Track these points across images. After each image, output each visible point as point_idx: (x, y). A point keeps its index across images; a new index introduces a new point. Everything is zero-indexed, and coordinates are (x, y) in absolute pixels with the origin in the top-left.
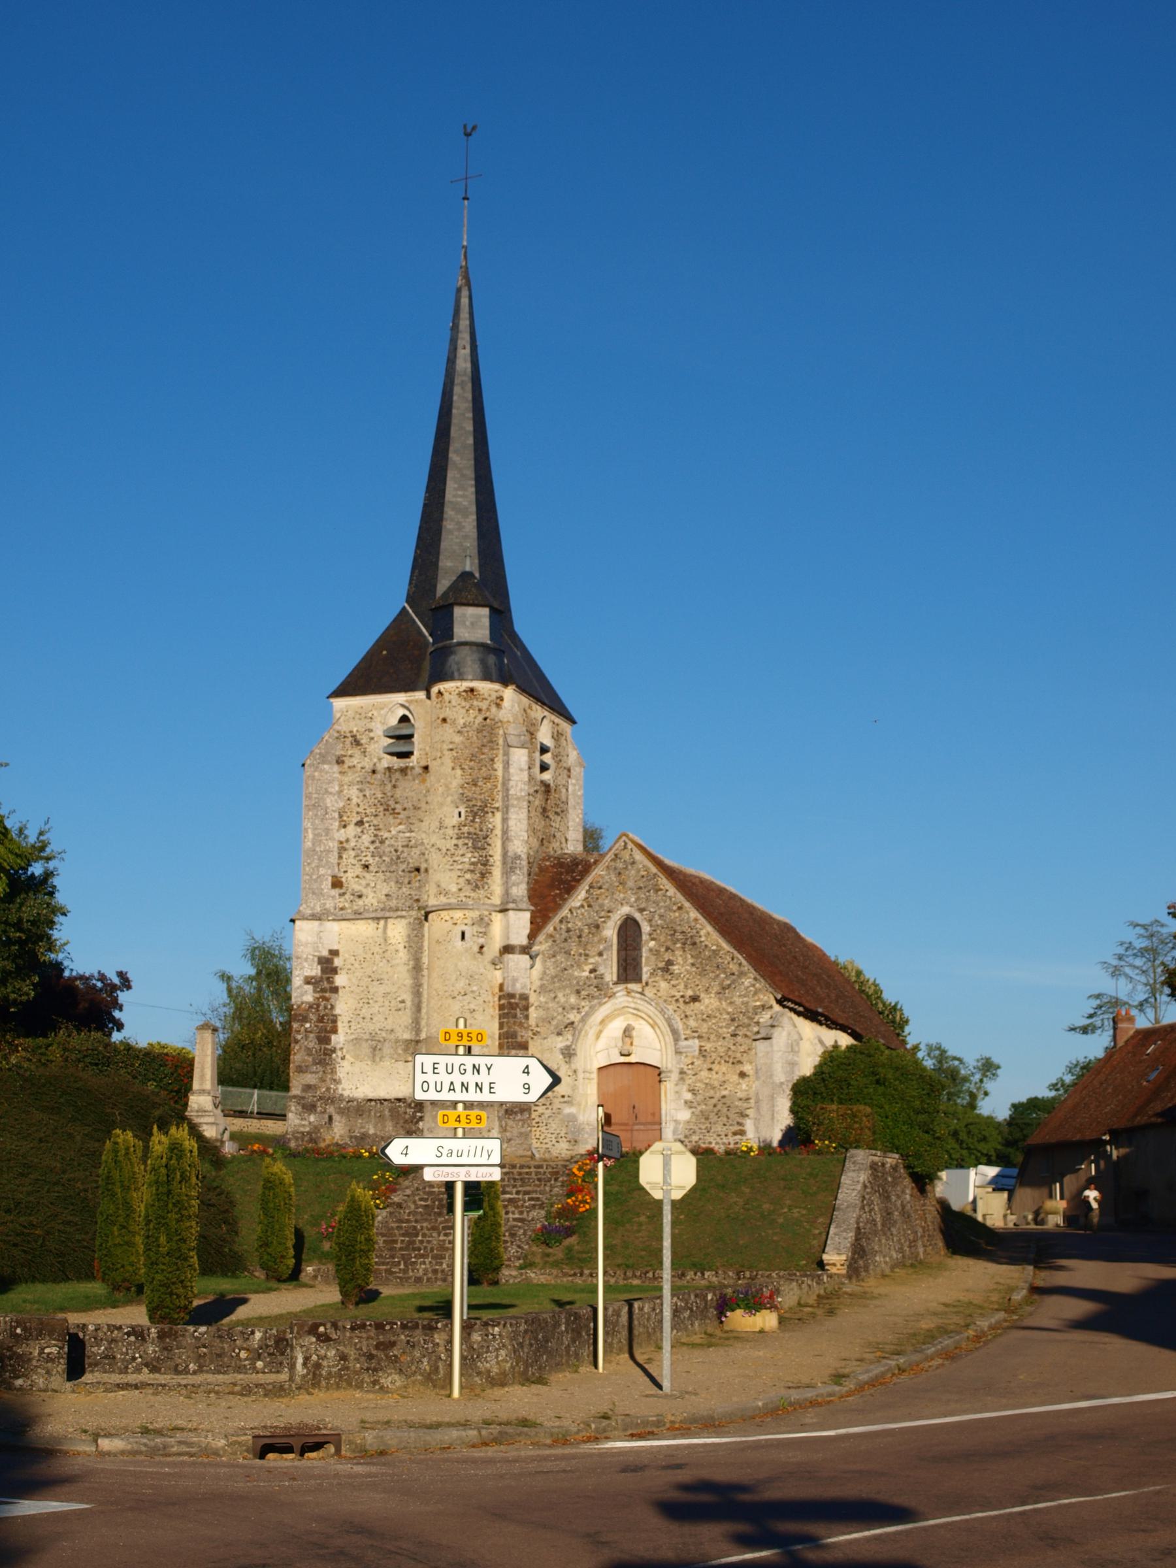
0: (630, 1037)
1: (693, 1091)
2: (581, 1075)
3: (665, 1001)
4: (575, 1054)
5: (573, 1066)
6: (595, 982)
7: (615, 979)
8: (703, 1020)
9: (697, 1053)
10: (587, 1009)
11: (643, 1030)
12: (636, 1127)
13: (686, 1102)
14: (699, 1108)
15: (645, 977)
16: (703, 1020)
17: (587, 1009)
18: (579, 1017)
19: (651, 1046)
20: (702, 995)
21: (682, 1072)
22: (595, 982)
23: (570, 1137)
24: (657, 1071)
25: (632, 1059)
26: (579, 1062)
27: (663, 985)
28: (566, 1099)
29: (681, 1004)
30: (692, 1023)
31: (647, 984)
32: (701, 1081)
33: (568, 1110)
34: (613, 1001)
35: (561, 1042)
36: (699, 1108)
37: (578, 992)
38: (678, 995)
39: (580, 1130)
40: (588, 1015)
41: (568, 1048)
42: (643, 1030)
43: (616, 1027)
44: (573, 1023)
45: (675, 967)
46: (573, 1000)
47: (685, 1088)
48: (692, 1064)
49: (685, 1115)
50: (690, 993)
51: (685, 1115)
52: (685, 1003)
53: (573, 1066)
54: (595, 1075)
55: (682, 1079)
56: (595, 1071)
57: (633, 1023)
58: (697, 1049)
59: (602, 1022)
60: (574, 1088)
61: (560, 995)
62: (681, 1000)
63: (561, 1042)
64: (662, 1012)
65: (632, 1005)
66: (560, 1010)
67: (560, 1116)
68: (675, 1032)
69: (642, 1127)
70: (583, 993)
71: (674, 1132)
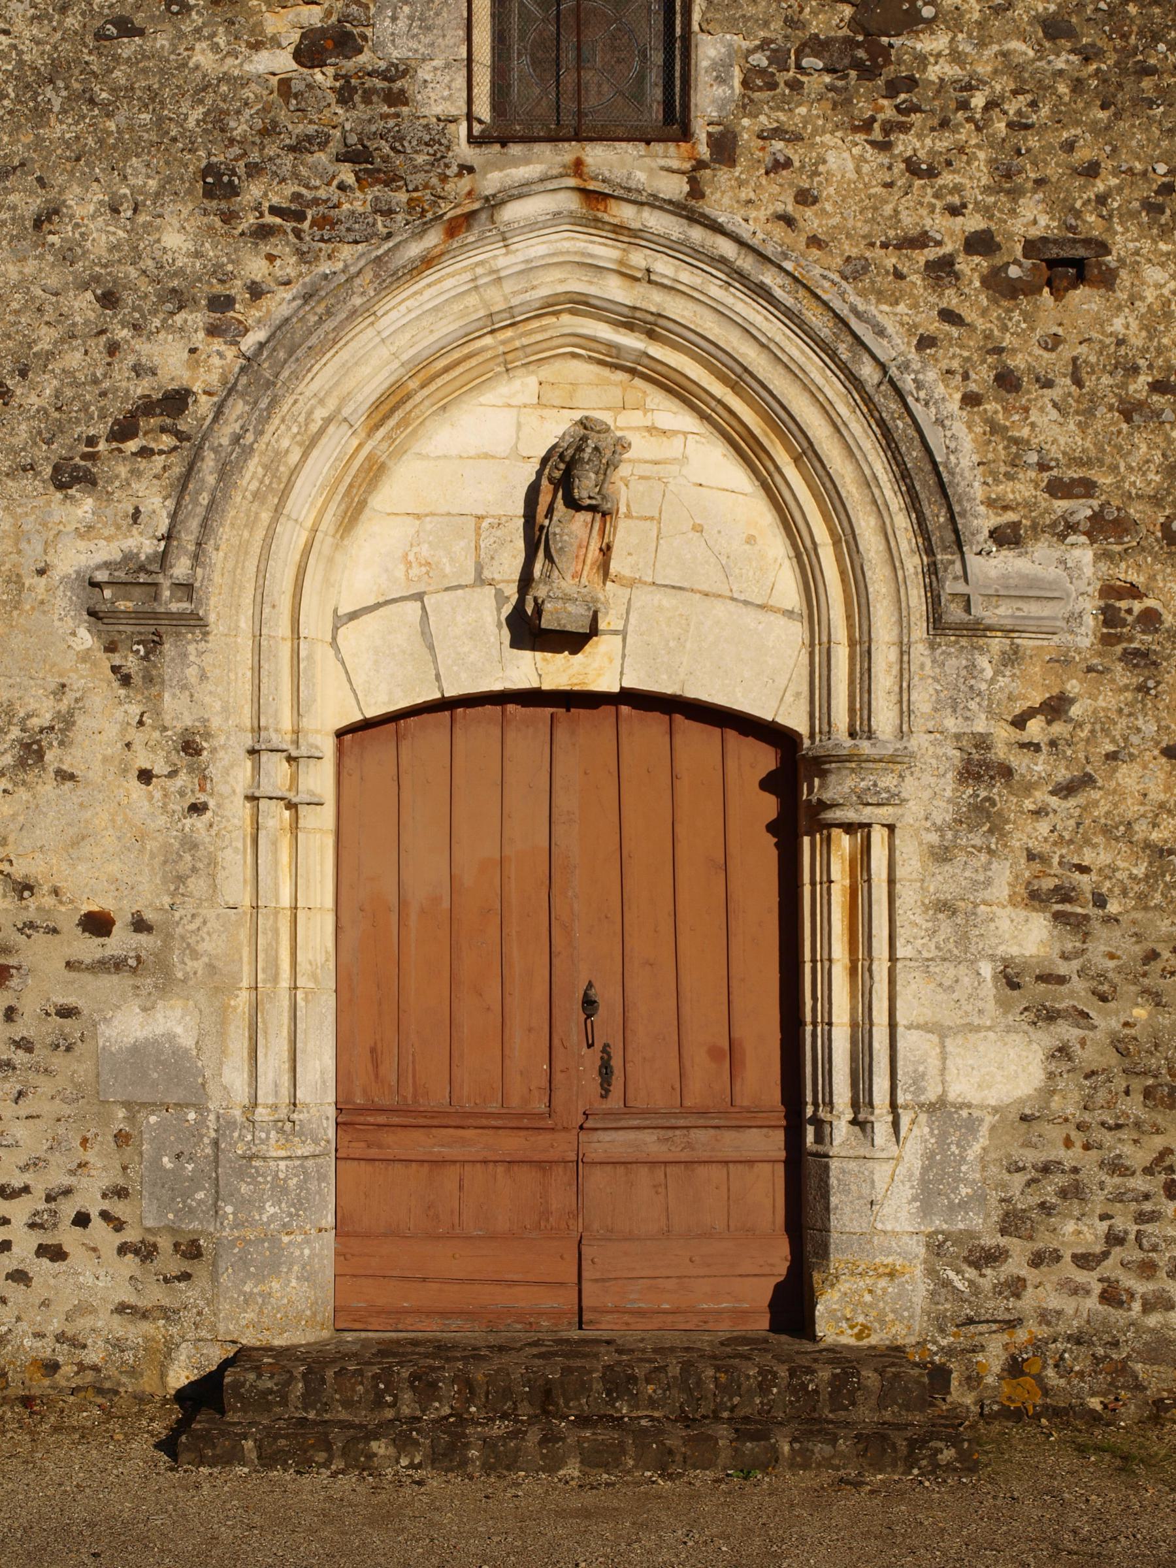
0: (601, 511)
1: (1054, 899)
2: (232, 775)
3: (855, 270)
4: (195, 622)
5: (177, 710)
6: (347, 120)
7: (483, 109)
8: (1128, 411)
9: (1085, 636)
10: (281, 303)
11: (685, 481)
12: (608, 1143)
13: (1010, 979)
14: (1107, 1022)
15: (710, 100)
16: (1128, 411)
17: (281, 303)
18: (221, 359)
19: (712, 596)
20: (1124, 241)
21: (979, 767)
22: (347, 120)
23: (144, 1216)
24: (765, 759)
25: (596, 669)
26: (215, 682)
27: (842, 159)
28: (121, 941)
29: (970, 296)
30: (1050, 428)
31: (724, 148)
32: (1117, 831)
33: (128, 1023)
34: (482, 256)
35: (83, 538)
36: (1107, 1022)
37: (218, 186)
38: (949, 232)
39: (222, 1166)
40: (292, 346)
41: (139, 575)
42: (685, 481)
43: (492, 440)
44: (176, 401)
45: (927, 44)
46: (177, 238)
47: (1004, 877)
48: (1055, 708)
49: (999, 1069)
50: (1032, 218)
51: (999, 1069)
52: (1000, 286)
53: (177, 710)
54: (320, 780)
55: (982, 816)
56: (327, 746)
57: (624, 423)
58: (1090, 606)
59: (391, 407)
60: (184, 865)
61: (83, 203)
62: (971, 267)
63: (83, 538)
64: (840, 344)
65: (615, 290)
66: (83, 306)
67: (78, 1068)
68: (924, 483)
69: (650, 1143)
70: (254, 191)
71: (930, 1192)
